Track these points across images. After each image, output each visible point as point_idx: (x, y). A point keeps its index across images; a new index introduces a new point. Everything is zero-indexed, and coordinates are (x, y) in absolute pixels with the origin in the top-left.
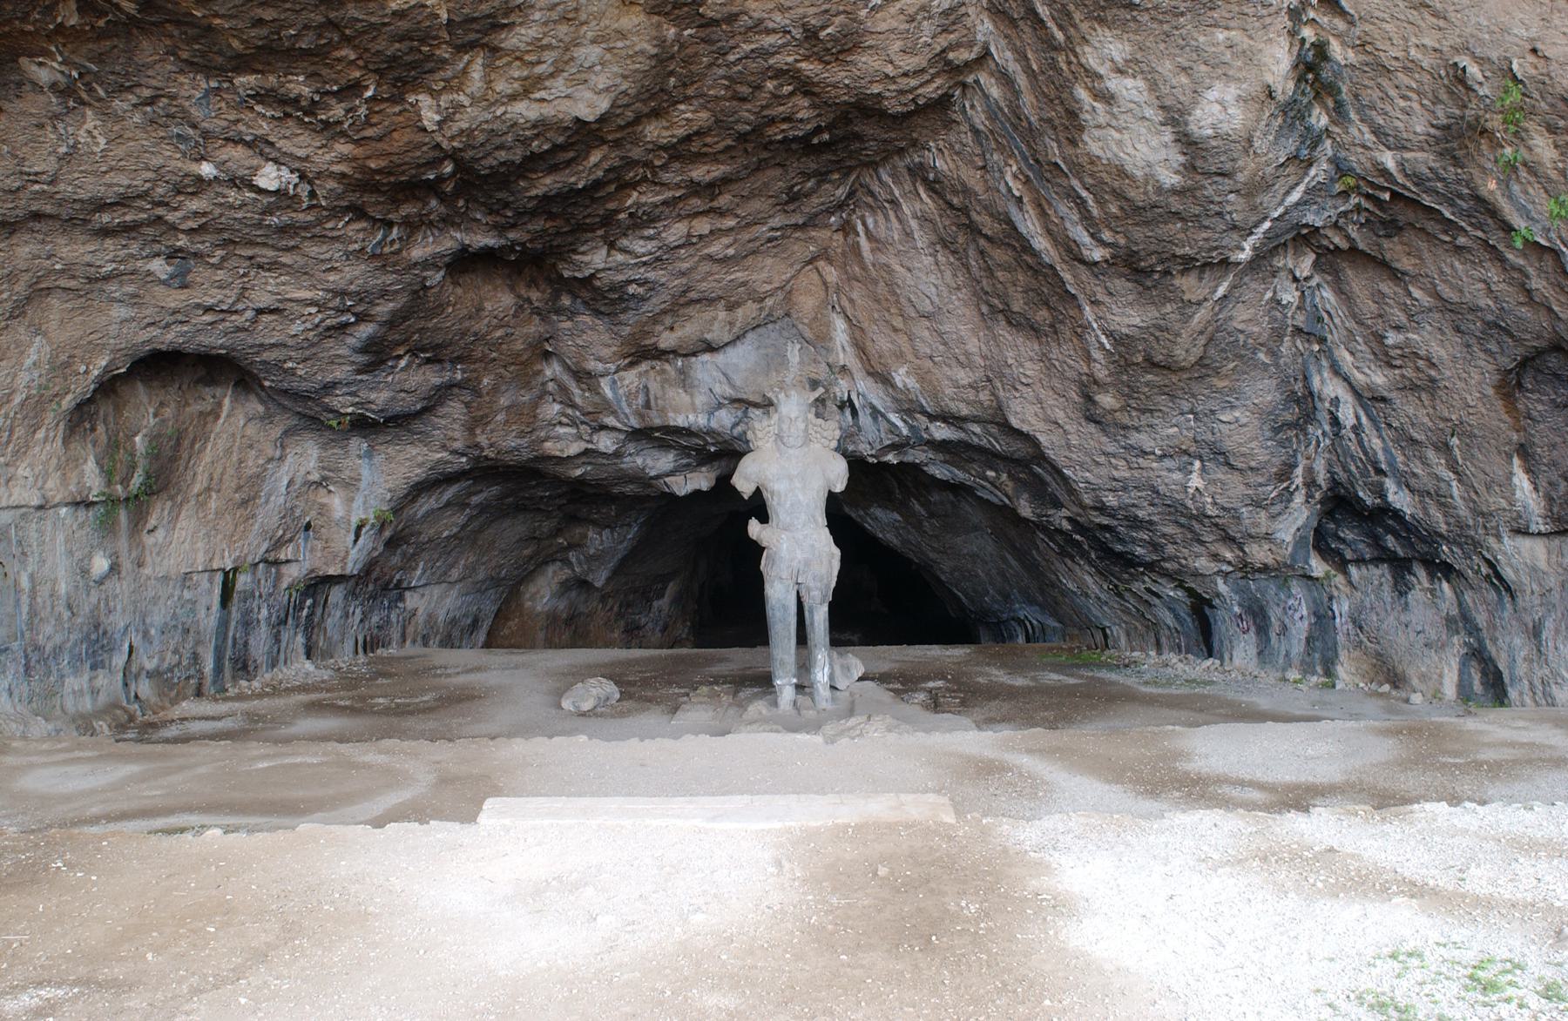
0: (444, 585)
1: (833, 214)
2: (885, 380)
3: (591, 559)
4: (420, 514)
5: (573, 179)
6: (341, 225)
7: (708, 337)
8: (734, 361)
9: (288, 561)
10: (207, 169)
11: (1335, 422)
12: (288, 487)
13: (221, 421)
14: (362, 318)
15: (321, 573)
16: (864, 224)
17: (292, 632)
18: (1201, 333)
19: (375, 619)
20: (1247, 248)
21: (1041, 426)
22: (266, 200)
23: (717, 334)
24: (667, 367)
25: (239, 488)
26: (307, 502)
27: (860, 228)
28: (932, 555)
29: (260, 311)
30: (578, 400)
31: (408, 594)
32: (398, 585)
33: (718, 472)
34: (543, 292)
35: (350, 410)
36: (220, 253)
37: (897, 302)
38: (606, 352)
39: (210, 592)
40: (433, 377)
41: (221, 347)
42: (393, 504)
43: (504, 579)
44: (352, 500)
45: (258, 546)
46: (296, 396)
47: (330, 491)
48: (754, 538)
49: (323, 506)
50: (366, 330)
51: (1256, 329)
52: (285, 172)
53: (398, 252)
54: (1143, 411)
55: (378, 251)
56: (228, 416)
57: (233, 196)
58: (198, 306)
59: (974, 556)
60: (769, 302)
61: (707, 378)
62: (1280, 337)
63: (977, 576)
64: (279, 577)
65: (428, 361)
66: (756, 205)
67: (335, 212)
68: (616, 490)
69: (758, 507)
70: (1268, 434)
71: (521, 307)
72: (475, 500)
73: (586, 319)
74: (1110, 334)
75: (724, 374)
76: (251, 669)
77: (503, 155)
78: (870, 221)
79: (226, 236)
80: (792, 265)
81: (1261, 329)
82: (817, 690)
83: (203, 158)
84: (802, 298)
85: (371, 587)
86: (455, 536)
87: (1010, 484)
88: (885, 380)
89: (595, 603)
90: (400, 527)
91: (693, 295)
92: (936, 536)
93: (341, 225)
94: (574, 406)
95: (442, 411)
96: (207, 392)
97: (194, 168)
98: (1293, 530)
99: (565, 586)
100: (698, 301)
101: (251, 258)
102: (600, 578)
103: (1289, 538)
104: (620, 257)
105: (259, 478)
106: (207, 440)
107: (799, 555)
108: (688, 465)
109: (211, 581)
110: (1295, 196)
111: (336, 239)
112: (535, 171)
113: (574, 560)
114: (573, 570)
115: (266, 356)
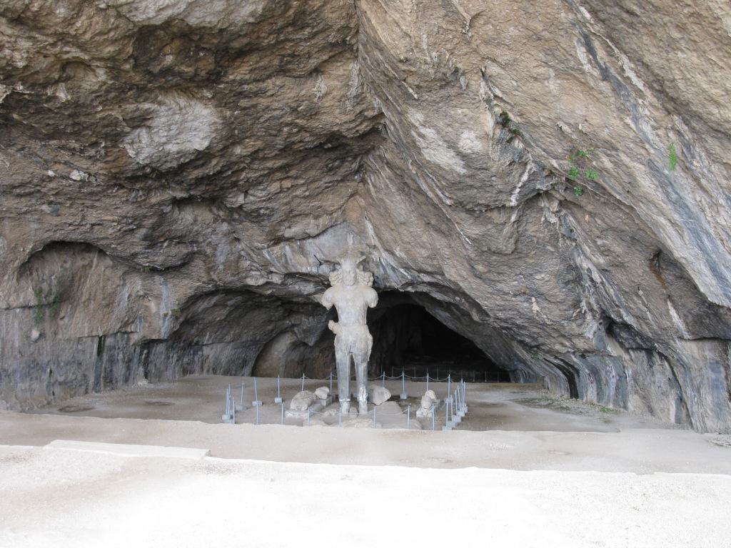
0: (223, 344)
1: (355, 175)
2: (392, 253)
3: (304, 331)
4: (200, 310)
5: (207, 171)
6: (114, 191)
7: (308, 231)
9: (132, 332)
10: (50, 173)
11: (592, 280)
12: (128, 298)
13: (93, 269)
14: (139, 227)
15: (148, 338)
16: (371, 180)
17: (137, 366)
18: (510, 238)
19: (186, 360)
20: (514, 200)
21: (459, 278)
22: (78, 184)
23: (312, 230)
24: (294, 245)
25: (104, 299)
26: (139, 305)
27: (369, 181)
29: (93, 225)
30: (256, 260)
31: (204, 348)
32: (197, 343)
34: (225, 212)
35: (147, 264)
36: (69, 202)
37: (390, 216)
38: (261, 239)
39: (92, 346)
40: (184, 250)
41: (81, 239)
42: (180, 306)
43: (259, 340)
44: (160, 304)
45: (116, 325)
46: (124, 259)
47: (150, 300)
48: (331, 329)
49: (147, 307)
50: (143, 231)
51: (541, 235)
52: (82, 173)
53: (145, 200)
54: (499, 274)
55: (135, 200)
56: (97, 266)
57: (64, 182)
58: (66, 223)
60: (335, 215)
61: (312, 250)
62: (557, 240)
63: (494, 347)
64: (129, 339)
65: (179, 243)
66: (312, 173)
67: (109, 187)
68: (294, 300)
69: (333, 314)
70: (562, 285)
71: (216, 219)
72: (230, 303)
73: (247, 224)
74: (469, 238)
76: (114, 382)
77: (169, 165)
78: (372, 178)
79: (69, 196)
80: (343, 198)
81: (545, 234)
83: (48, 169)
84: (351, 213)
85: (182, 344)
86: (224, 320)
87: (467, 304)
88: (392, 253)
90: (189, 317)
91: (295, 213)
93: (114, 191)
94: (255, 262)
95: (193, 264)
96: (87, 255)
97: (45, 172)
98: (592, 332)
99: (295, 346)
100: (300, 215)
101: (83, 204)
103: (591, 337)
104: (252, 198)
105: (114, 294)
106: (87, 277)
107: (351, 339)
109: (92, 341)
110: (525, 177)
111: (115, 196)
112: (188, 169)
113: (297, 332)
115: (101, 242)
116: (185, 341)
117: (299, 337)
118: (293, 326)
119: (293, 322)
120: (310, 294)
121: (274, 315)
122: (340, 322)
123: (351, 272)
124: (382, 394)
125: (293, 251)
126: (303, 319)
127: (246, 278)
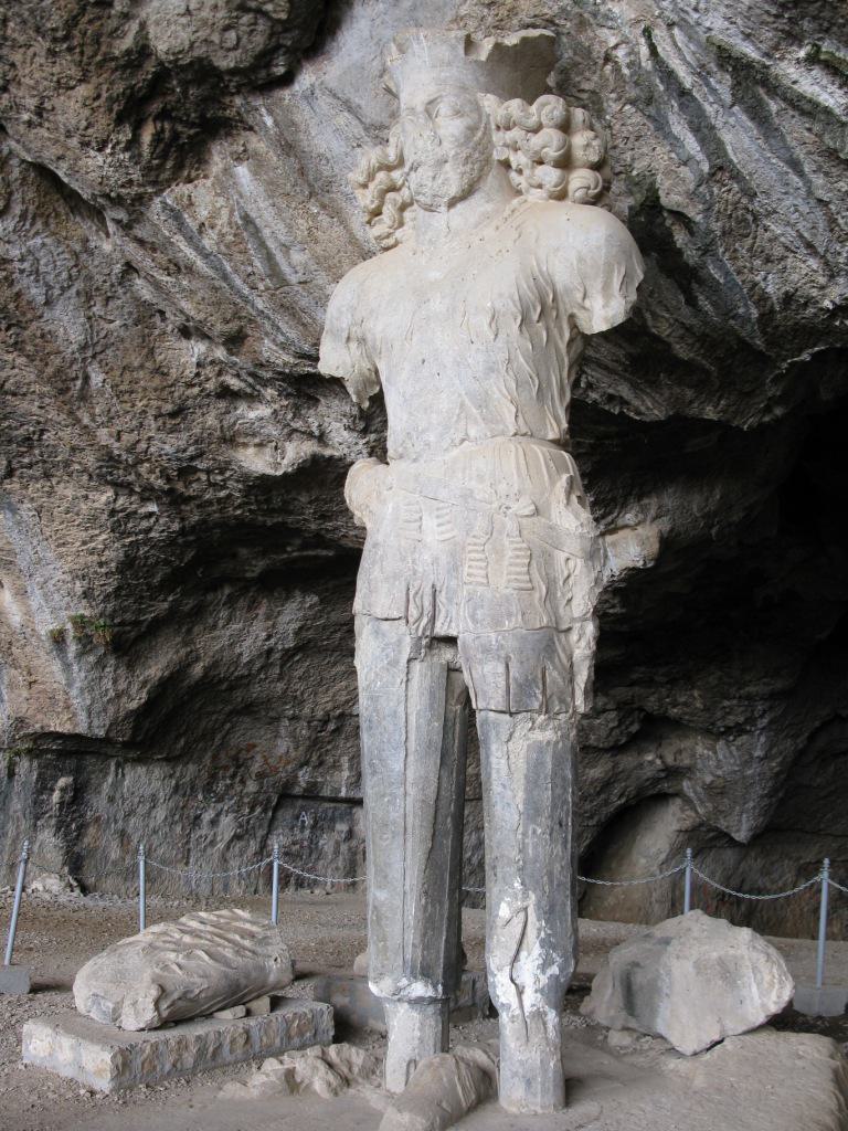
3: (716, 791)
4: (248, 648)
24: (257, 143)
32: (312, 794)
33: (665, 525)
85: (252, 787)
116: (261, 776)
117: (701, 810)
119: (670, 760)
123: (444, 108)
125: (272, 188)
126: (700, 749)
127: (230, 440)
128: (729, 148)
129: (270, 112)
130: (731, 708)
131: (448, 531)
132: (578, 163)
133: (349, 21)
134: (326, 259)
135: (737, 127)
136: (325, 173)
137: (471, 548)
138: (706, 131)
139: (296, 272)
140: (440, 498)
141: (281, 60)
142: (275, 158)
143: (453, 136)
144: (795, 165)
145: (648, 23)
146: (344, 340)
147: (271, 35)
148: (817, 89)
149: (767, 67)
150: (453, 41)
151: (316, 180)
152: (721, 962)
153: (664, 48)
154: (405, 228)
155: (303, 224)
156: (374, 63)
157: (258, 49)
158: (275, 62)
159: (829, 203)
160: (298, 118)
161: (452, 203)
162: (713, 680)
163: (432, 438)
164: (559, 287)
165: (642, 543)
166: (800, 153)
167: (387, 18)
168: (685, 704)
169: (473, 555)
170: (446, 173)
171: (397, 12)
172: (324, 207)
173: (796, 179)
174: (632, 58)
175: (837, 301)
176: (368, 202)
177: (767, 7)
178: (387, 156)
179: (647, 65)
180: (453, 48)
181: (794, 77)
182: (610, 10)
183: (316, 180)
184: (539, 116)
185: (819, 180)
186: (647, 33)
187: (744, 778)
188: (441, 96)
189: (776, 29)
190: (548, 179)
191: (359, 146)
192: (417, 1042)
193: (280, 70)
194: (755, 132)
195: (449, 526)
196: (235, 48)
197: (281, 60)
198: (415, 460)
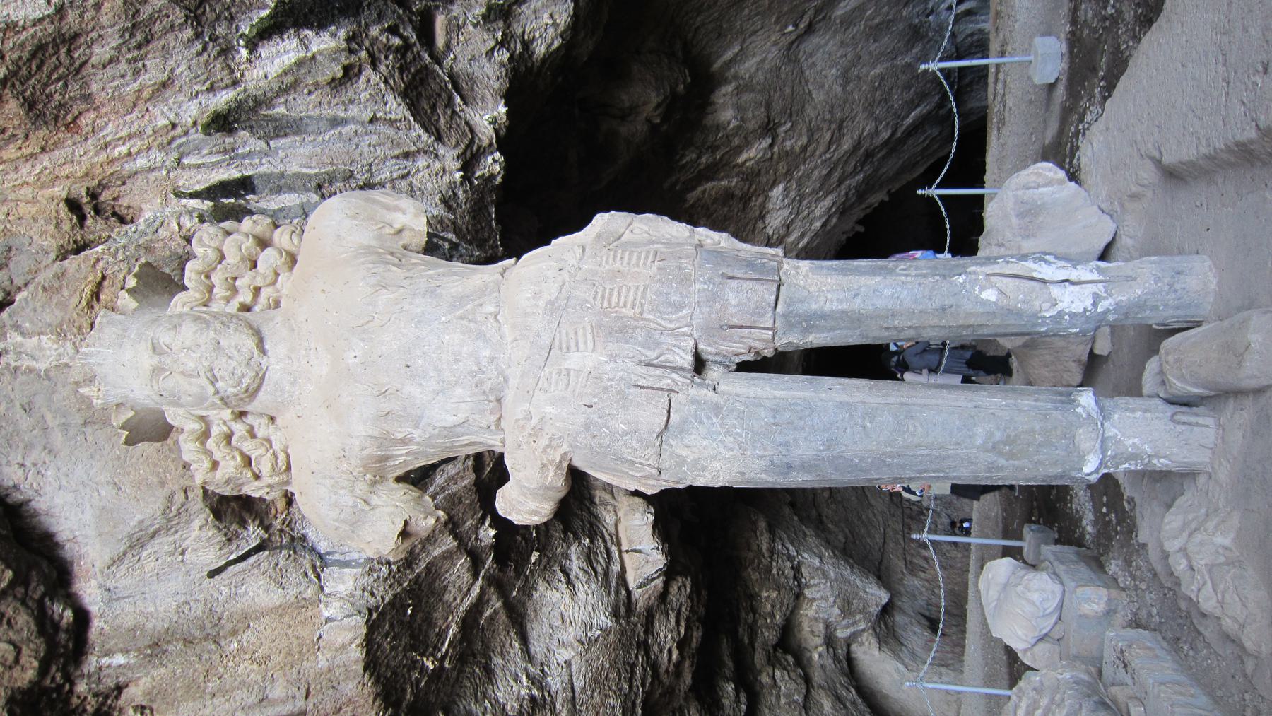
8: (88, 516)
28: (847, 145)
59: (845, 76)
61: (176, 583)
63: (882, 78)
75: (138, 543)
82: (1125, 310)
89: (917, 583)
92: (811, 133)
102: (878, 596)
108: (589, 556)
113: (848, 632)
114: (863, 630)
117: (862, 626)
118: (830, 641)
120: (623, 607)
121: (788, 696)
122: (491, 441)
123: (165, 338)
124: (1030, 213)
126: (811, 613)
128: (305, 170)
129: (108, 653)
130: (778, 569)
131: (585, 335)
132: (267, 235)
133: (53, 520)
134: (289, 653)
135: (289, 152)
136: (199, 612)
137: (605, 305)
138: (284, 181)
139: (294, 697)
140: (548, 342)
141: (58, 608)
142: (163, 671)
143: (196, 332)
144: (335, 122)
145: (170, 189)
146: (367, 508)
147: (24, 602)
148: (277, 61)
149: (245, 90)
150: (105, 320)
151: (202, 628)
152: (1021, 215)
153: (198, 182)
154: (273, 438)
155: (245, 667)
156: (104, 494)
157: (33, 627)
158: (56, 617)
159: (375, 115)
160: (129, 622)
161: (264, 352)
162: (755, 576)
163: (487, 353)
164: (374, 243)
165: (633, 510)
166: (328, 112)
167: (64, 469)
168: (773, 606)
169: (614, 301)
170: (230, 346)
171: (62, 455)
172: (234, 632)
173: (347, 128)
174: (195, 214)
175: (458, 165)
176: (232, 463)
177: (194, 51)
178: (194, 431)
179: (206, 205)
180: (111, 323)
181: (261, 73)
182: (145, 221)
183: (202, 628)
184: (210, 247)
185: (354, 111)
186: (179, 195)
187: (836, 580)
188: (152, 339)
189: (216, 59)
190: (272, 261)
191: (183, 553)
192: (1148, 415)
193: (68, 615)
194: (297, 138)
195: (580, 333)
196: (18, 651)
197: (58, 608)
198: (506, 380)
